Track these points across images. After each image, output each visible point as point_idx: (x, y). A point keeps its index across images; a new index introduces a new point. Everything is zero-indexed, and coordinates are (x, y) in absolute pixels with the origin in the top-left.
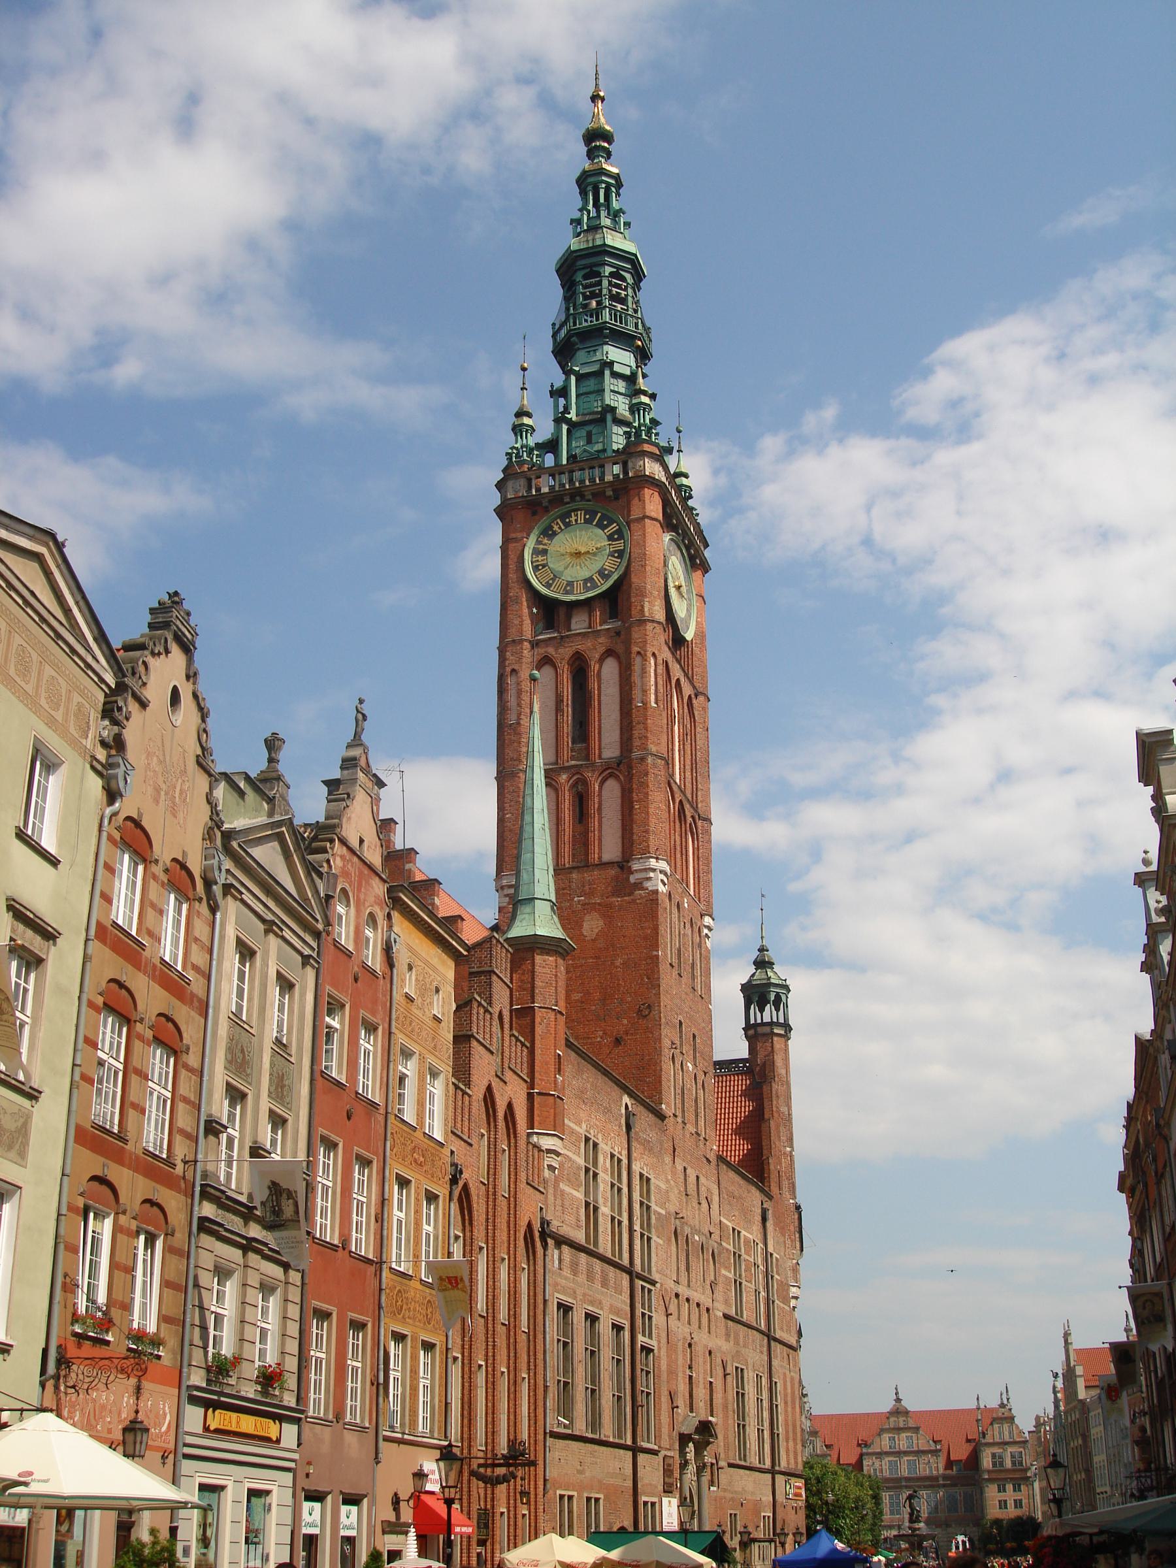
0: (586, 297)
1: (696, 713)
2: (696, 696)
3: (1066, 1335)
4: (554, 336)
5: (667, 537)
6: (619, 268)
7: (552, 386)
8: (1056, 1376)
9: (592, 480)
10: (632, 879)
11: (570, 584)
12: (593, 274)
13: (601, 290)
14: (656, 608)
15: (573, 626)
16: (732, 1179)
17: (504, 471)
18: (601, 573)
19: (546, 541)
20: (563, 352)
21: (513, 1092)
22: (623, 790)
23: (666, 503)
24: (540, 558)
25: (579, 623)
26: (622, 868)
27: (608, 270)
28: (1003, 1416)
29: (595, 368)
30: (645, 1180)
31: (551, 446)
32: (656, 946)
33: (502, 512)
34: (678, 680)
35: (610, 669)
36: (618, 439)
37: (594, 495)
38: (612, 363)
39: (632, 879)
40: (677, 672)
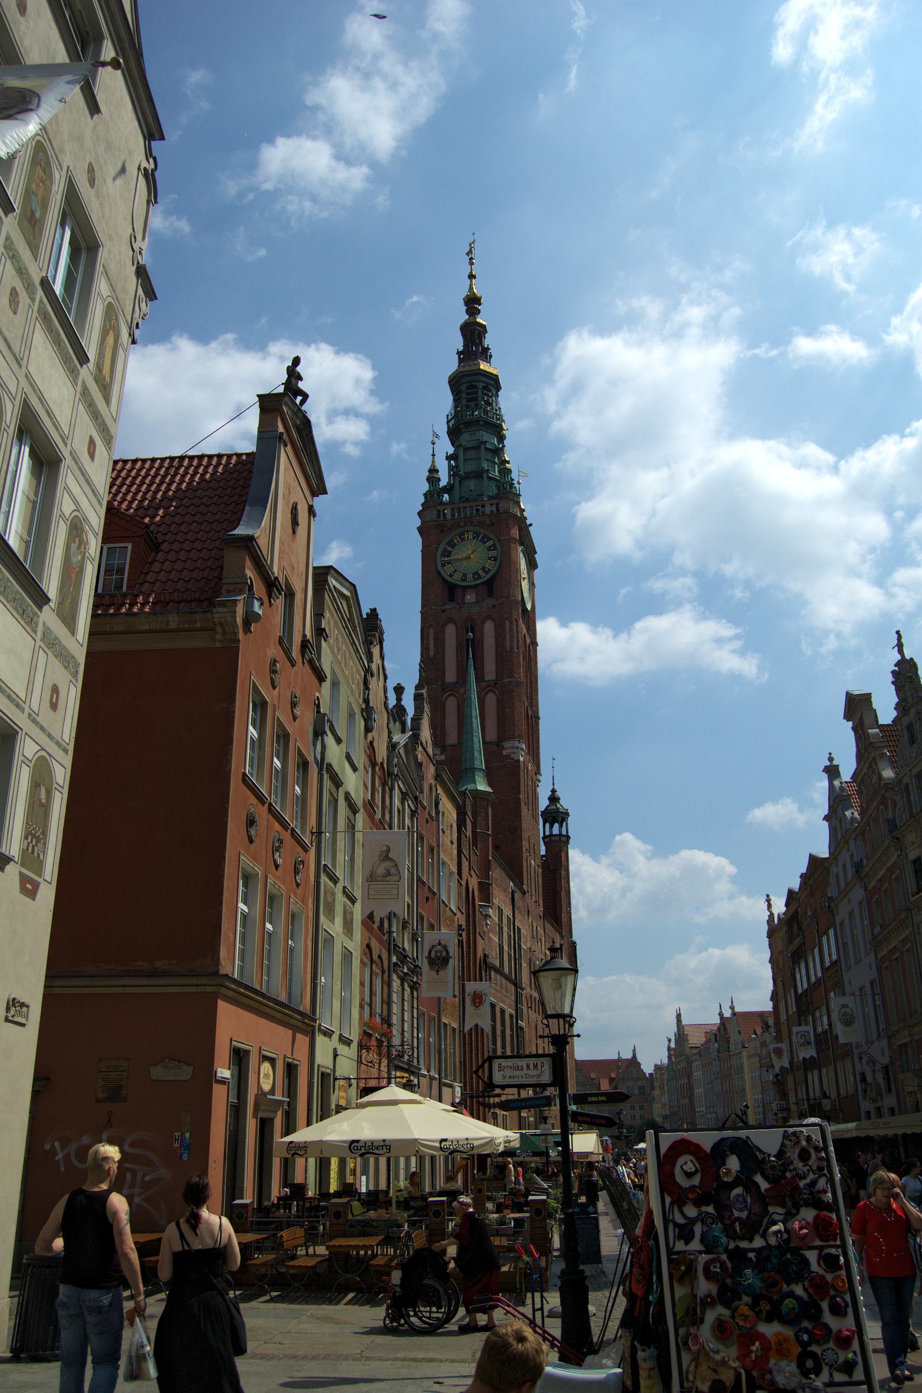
0: (468, 401)
3: (679, 1017)
4: (448, 422)
5: (520, 548)
6: (488, 384)
8: (670, 1040)
10: (504, 753)
11: (465, 575)
12: (472, 387)
13: (477, 398)
16: (548, 926)
17: (422, 505)
20: (454, 434)
21: (474, 883)
22: (498, 700)
23: (520, 529)
24: (446, 559)
25: (470, 597)
26: (498, 745)
27: (483, 384)
28: (633, 1063)
29: (475, 444)
30: (519, 929)
31: (448, 489)
32: (519, 792)
33: (420, 530)
35: (489, 628)
36: (492, 490)
38: (485, 442)
39: (504, 753)
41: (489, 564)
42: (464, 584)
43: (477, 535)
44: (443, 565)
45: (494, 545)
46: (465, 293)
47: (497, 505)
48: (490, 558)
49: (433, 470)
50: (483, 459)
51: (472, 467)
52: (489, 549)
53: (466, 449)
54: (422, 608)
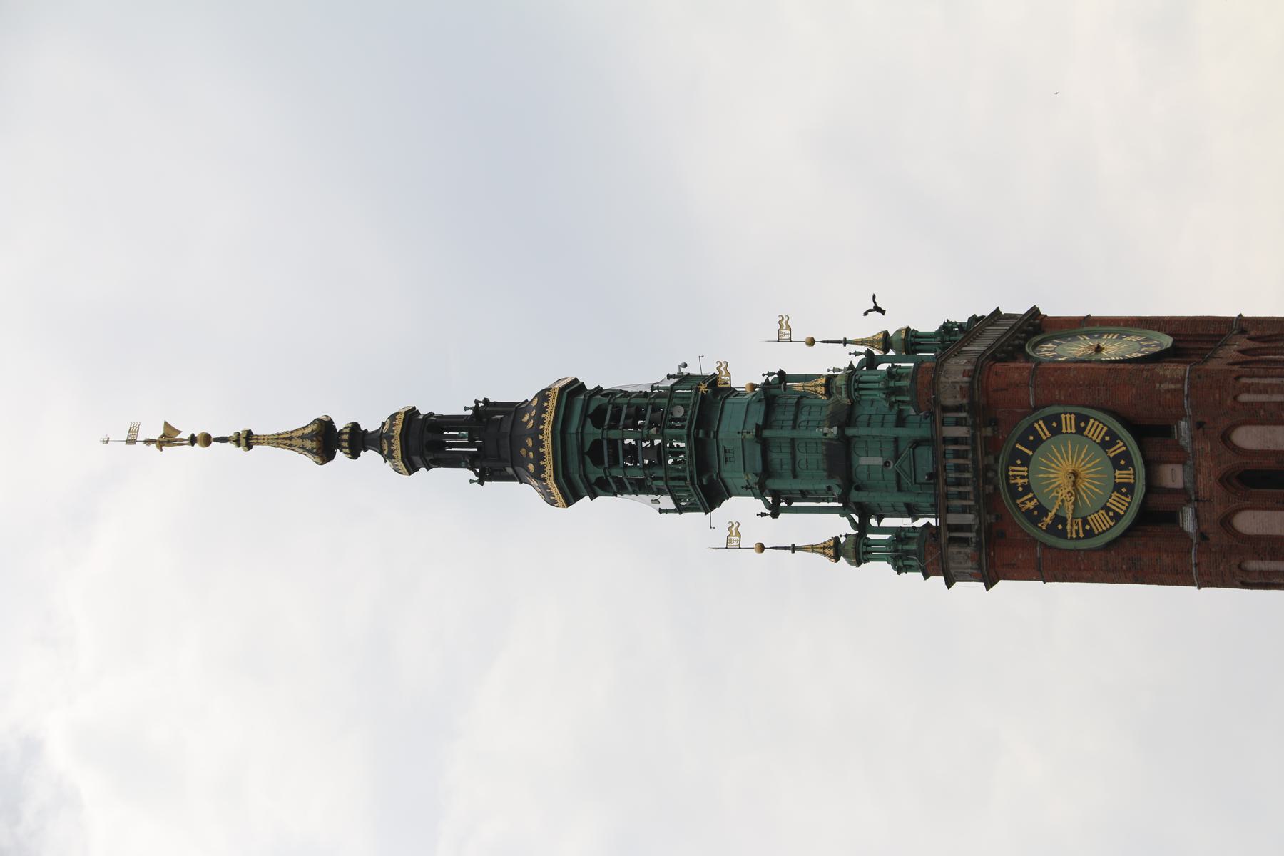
1: (1268, 332)
2: (1243, 331)
4: (680, 510)
6: (585, 414)
7: (763, 515)
9: (957, 454)
14: (1168, 373)
15: (1179, 484)
18: (1105, 445)
19: (1048, 520)
23: (994, 358)
25: (1173, 476)
27: (589, 427)
31: (864, 513)
34: (1240, 351)
35: (1249, 438)
37: (987, 454)
40: (1230, 352)
41: (1096, 429)
42: (1140, 490)
43: (1017, 457)
44: (1089, 534)
45: (1047, 421)
46: (304, 463)
47: (945, 409)
48: (1080, 431)
49: (836, 549)
50: (795, 434)
51: (812, 459)
52: (1056, 431)
53: (767, 472)
54: (1193, 584)
